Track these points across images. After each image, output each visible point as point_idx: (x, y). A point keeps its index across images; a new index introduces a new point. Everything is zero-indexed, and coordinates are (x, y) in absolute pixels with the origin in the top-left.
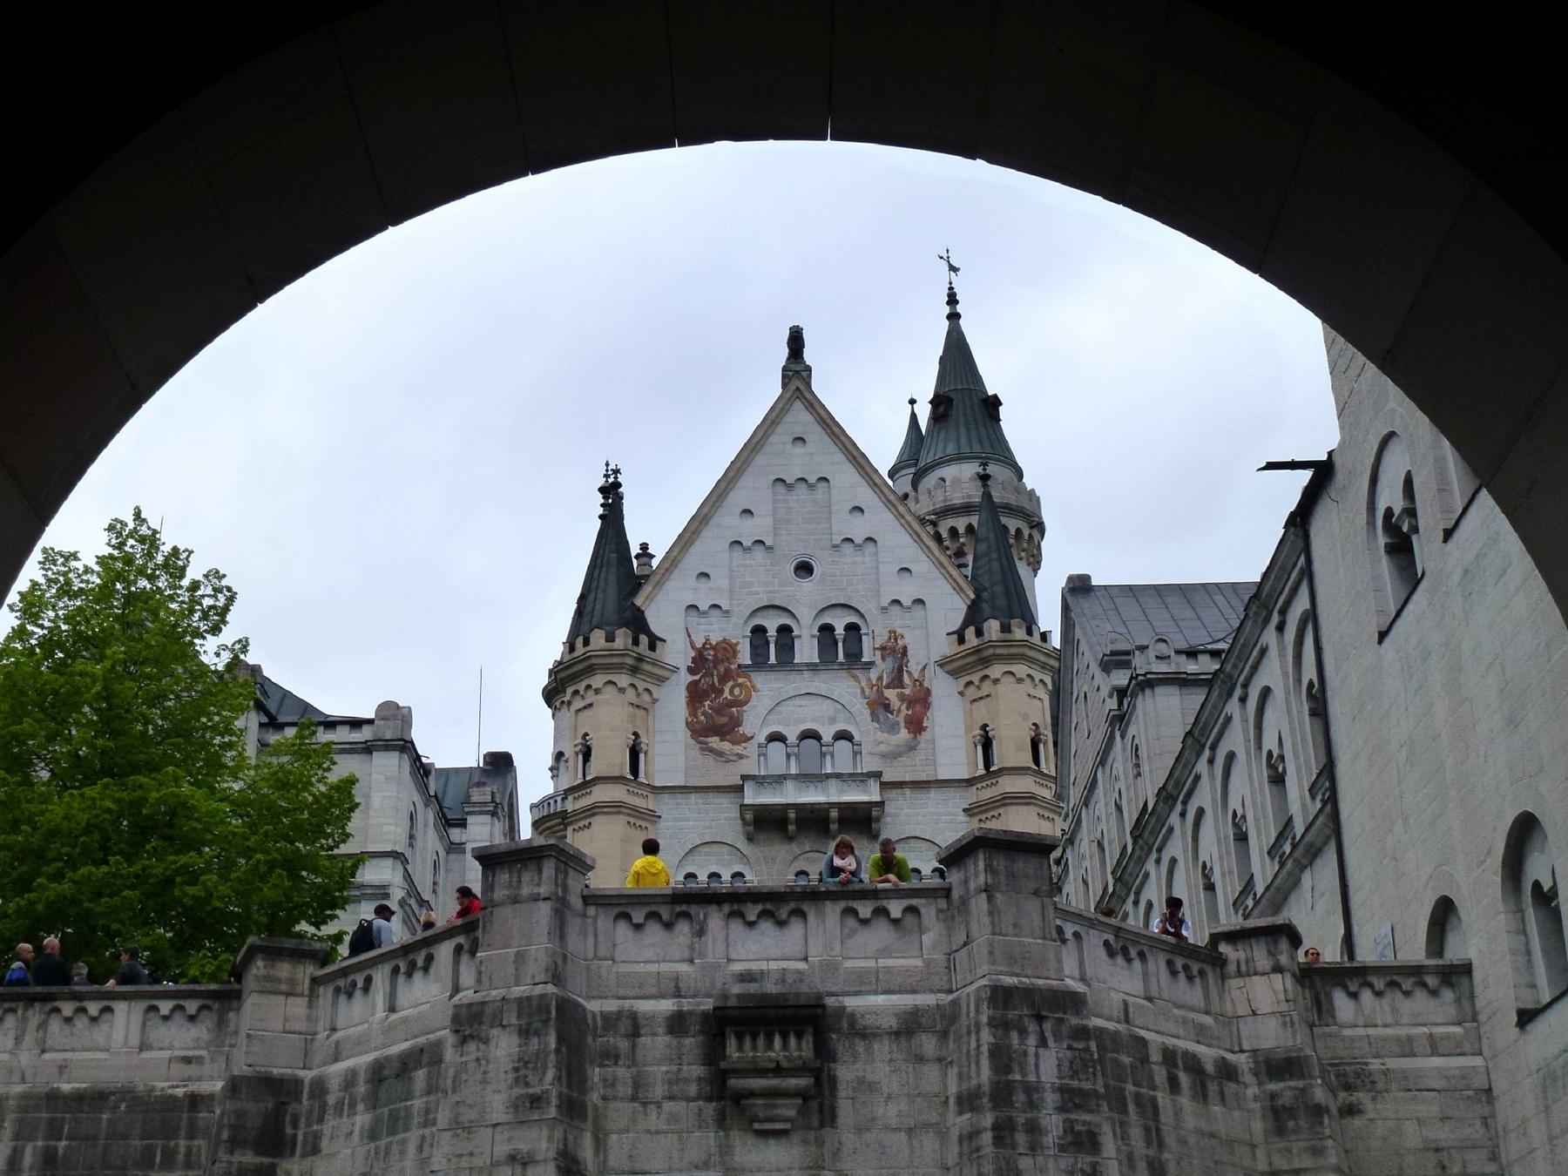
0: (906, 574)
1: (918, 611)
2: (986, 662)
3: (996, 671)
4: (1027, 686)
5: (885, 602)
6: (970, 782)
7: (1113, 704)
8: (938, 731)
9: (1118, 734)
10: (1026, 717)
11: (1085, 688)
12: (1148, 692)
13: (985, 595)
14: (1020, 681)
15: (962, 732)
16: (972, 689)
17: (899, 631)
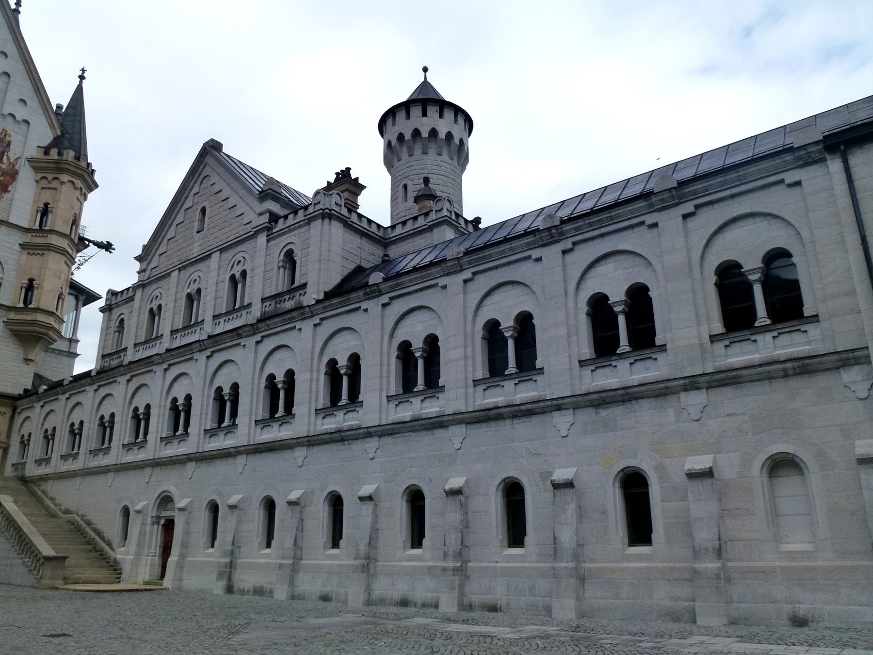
0: (22, 104)
1: (24, 127)
2: (60, 170)
3: (65, 178)
4: (77, 193)
5: (6, 112)
6: (28, 230)
7: (266, 218)
8: (17, 195)
9: (262, 239)
10: (73, 208)
11: (205, 204)
12: (327, 221)
13: (67, 136)
14: (76, 188)
15: (31, 202)
16: (44, 183)
17: (9, 131)
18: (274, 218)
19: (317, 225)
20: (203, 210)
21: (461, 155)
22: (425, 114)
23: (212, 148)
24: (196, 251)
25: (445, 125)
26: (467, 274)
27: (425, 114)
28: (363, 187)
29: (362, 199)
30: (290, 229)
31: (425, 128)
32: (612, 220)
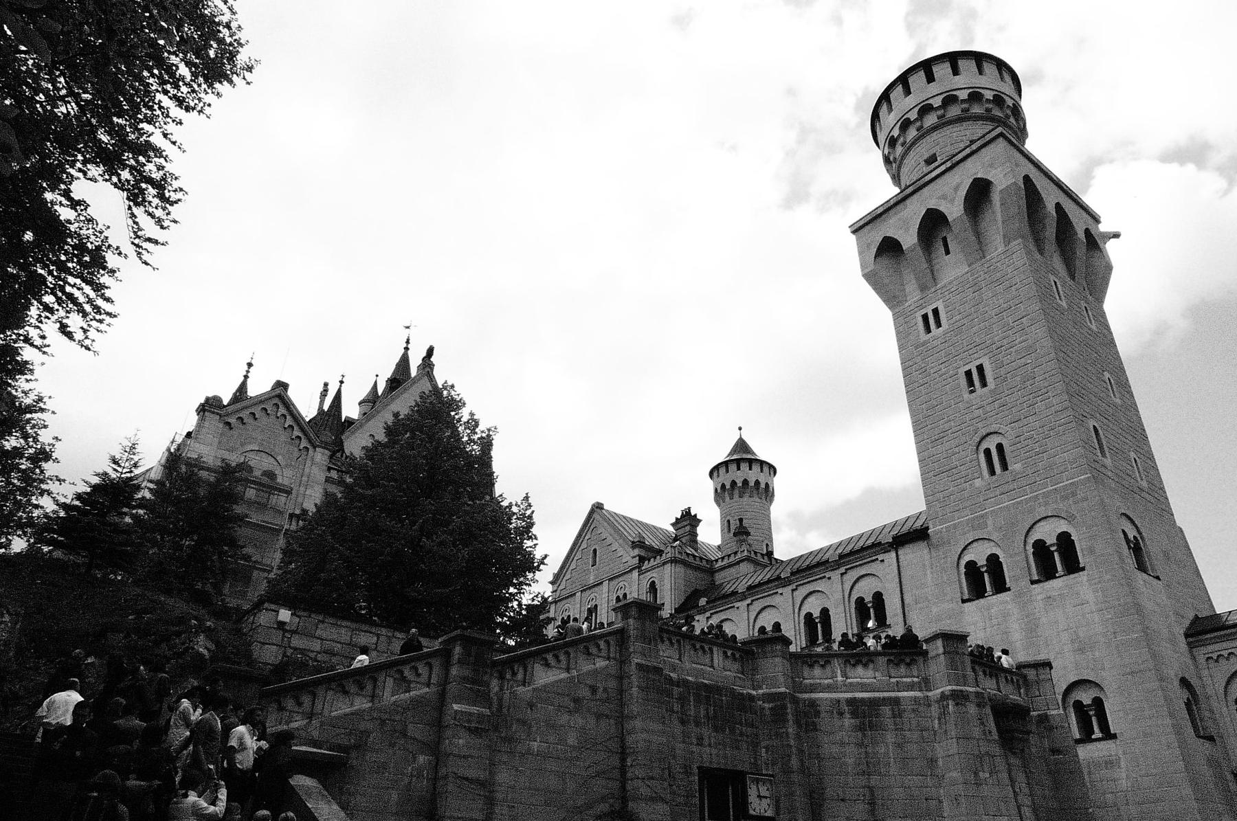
9: (635, 573)
18: (642, 559)
19: (668, 567)
20: (595, 551)
21: (767, 493)
22: (739, 469)
23: (598, 507)
24: (592, 580)
25: (753, 475)
26: (749, 601)
27: (739, 469)
28: (700, 521)
29: (699, 530)
30: (653, 568)
31: (744, 477)
32: (811, 575)
